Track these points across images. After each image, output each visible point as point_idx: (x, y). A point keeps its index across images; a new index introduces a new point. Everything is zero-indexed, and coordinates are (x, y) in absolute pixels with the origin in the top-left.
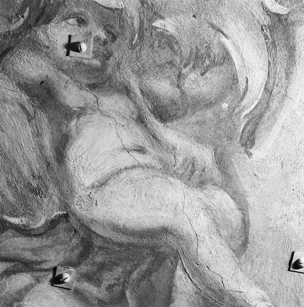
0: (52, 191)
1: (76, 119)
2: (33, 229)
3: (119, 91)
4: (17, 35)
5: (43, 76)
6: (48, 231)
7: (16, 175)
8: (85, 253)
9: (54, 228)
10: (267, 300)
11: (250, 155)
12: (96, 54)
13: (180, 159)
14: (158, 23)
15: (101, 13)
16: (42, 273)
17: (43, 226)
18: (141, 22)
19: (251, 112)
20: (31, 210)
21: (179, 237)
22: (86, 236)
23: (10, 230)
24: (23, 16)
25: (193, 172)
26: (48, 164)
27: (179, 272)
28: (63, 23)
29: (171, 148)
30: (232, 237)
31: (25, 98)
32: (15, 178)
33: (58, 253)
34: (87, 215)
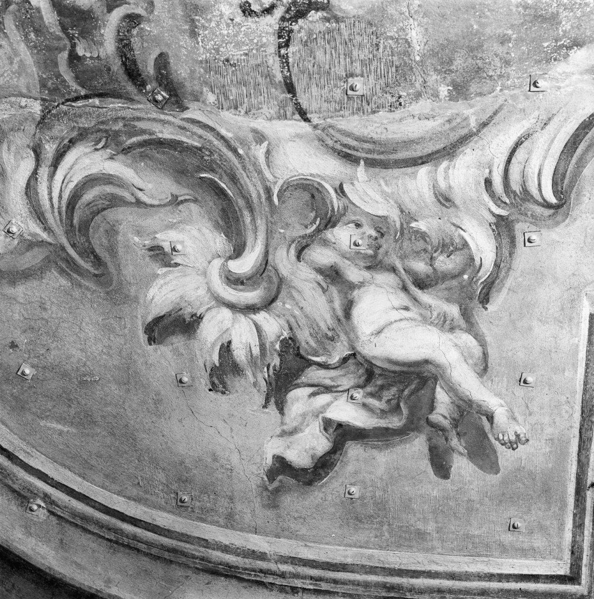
2: (330, 365)
3: (388, 270)
4: (311, 236)
11: (486, 309)
12: (370, 246)
13: (435, 314)
14: (413, 225)
15: (372, 219)
17: (338, 362)
18: (402, 224)
19: (485, 280)
21: (437, 366)
22: (369, 368)
25: (445, 322)
26: (339, 320)
27: (438, 389)
28: (345, 227)
29: (428, 306)
30: (476, 365)
31: (320, 278)
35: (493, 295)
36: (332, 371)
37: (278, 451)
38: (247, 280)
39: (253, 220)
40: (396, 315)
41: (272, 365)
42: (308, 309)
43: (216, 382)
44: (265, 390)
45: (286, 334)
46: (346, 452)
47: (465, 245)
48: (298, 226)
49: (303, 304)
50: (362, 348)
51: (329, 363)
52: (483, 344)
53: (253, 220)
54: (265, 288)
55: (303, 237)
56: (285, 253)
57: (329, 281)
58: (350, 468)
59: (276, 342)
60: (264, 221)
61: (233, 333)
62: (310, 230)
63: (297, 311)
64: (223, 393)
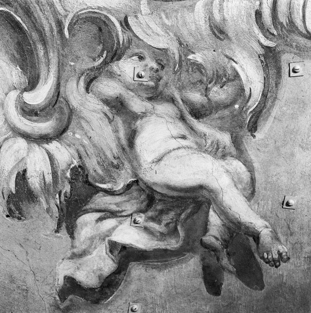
0: (127, 166)
1: (140, 119)
2: (115, 191)
3: (168, 101)
4: (99, 68)
5: (118, 94)
6: (125, 191)
7: (103, 157)
8: (150, 204)
9: (129, 189)
10: (269, 227)
11: (254, 137)
12: (151, 78)
13: (209, 142)
14: (191, 57)
15: (154, 52)
16: (123, 218)
17: (122, 188)
18: (180, 57)
19: (254, 109)
20: (113, 179)
21: (211, 191)
22: (150, 193)
23: (101, 192)
24: (102, 57)
25: (217, 149)
26: (124, 149)
27: (211, 213)
28: (129, 60)
29: (203, 135)
30: (244, 189)
31: (106, 108)
32: (102, 159)
33: (132, 205)
34: (150, 180)
35: (261, 122)
36: (117, 197)
37: (68, 273)
38: (41, 111)
39: (46, 53)
40: (175, 143)
41: (63, 192)
42: (96, 139)
43: (13, 208)
44: (57, 215)
45: (76, 163)
46: (130, 272)
47: (237, 76)
48: (87, 59)
49: (91, 133)
50: (144, 175)
51: (114, 189)
52: (251, 169)
53: (46, 53)
54: (57, 119)
55: (91, 70)
56: (75, 85)
57: (114, 111)
58: (133, 287)
59: (67, 170)
60: (56, 54)
61: (28, 161)
63: (86, 140)
64: (19, 219)
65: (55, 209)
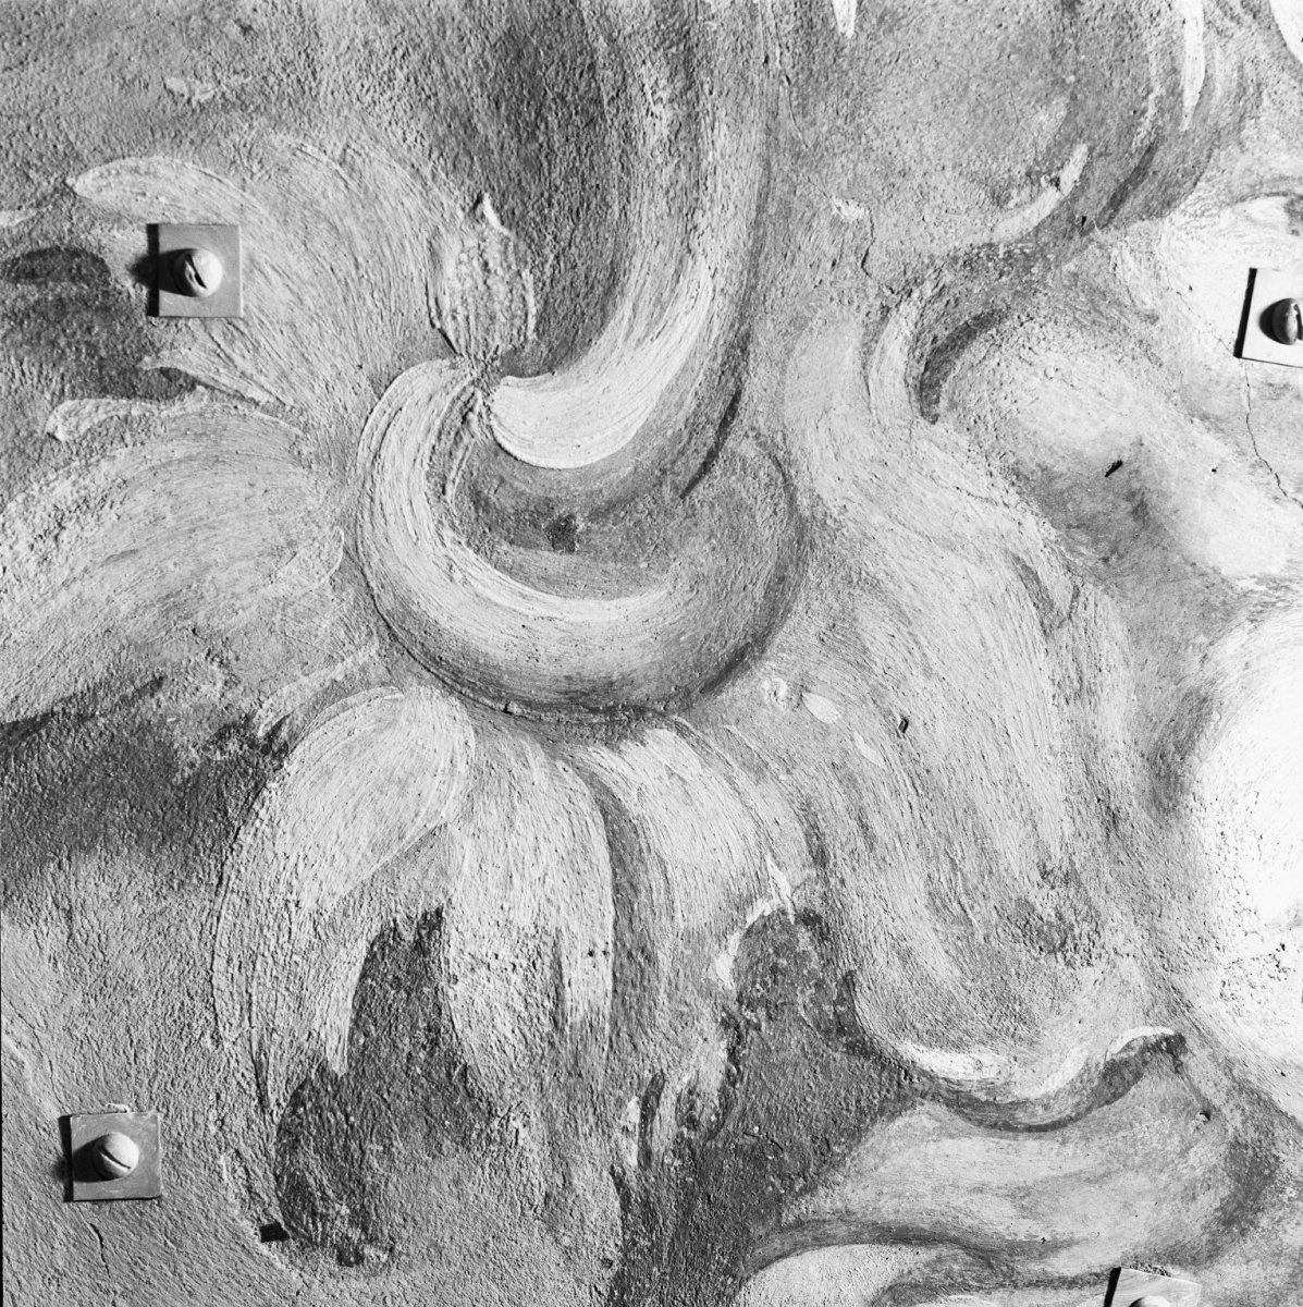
0: (1120, 939)
1: (1249, 626)
4: (1021, 261)
5: (1122, 442)
6: (1089, 1110)
7: (970, 866)
8: (1240, 1206)
9: (1116, 1096)
16: (1050, 1293)
20: (1022, 1020)
22: (1252, 1135)
23: (928, 1105)
24: (1056, 182)
26: (1113, 819)
31: (1035, 533)
32: (965, 879)
33: (1126, 1205)
34: (1264, 1045)
36: (1030, 1144)
38: (596, 515)
39: (689, 128)
41: (676, 1085)
42: (939, 736)
43: (317, 1174)
44: (613, 1253)
45: (786, 891)
48: (946, 185)
49: (922, 696)
50: (1222, 1008)
51: (1019, 1093)
54: (697, 581)
56: (849, 355)
57: (1088, 556)
59: (722, 937)
60: (755, 136)
61: (465, 853)
62: (1012, 226)
63: (870, 741)
64: (348, 1257)
65: (599, 1206)
